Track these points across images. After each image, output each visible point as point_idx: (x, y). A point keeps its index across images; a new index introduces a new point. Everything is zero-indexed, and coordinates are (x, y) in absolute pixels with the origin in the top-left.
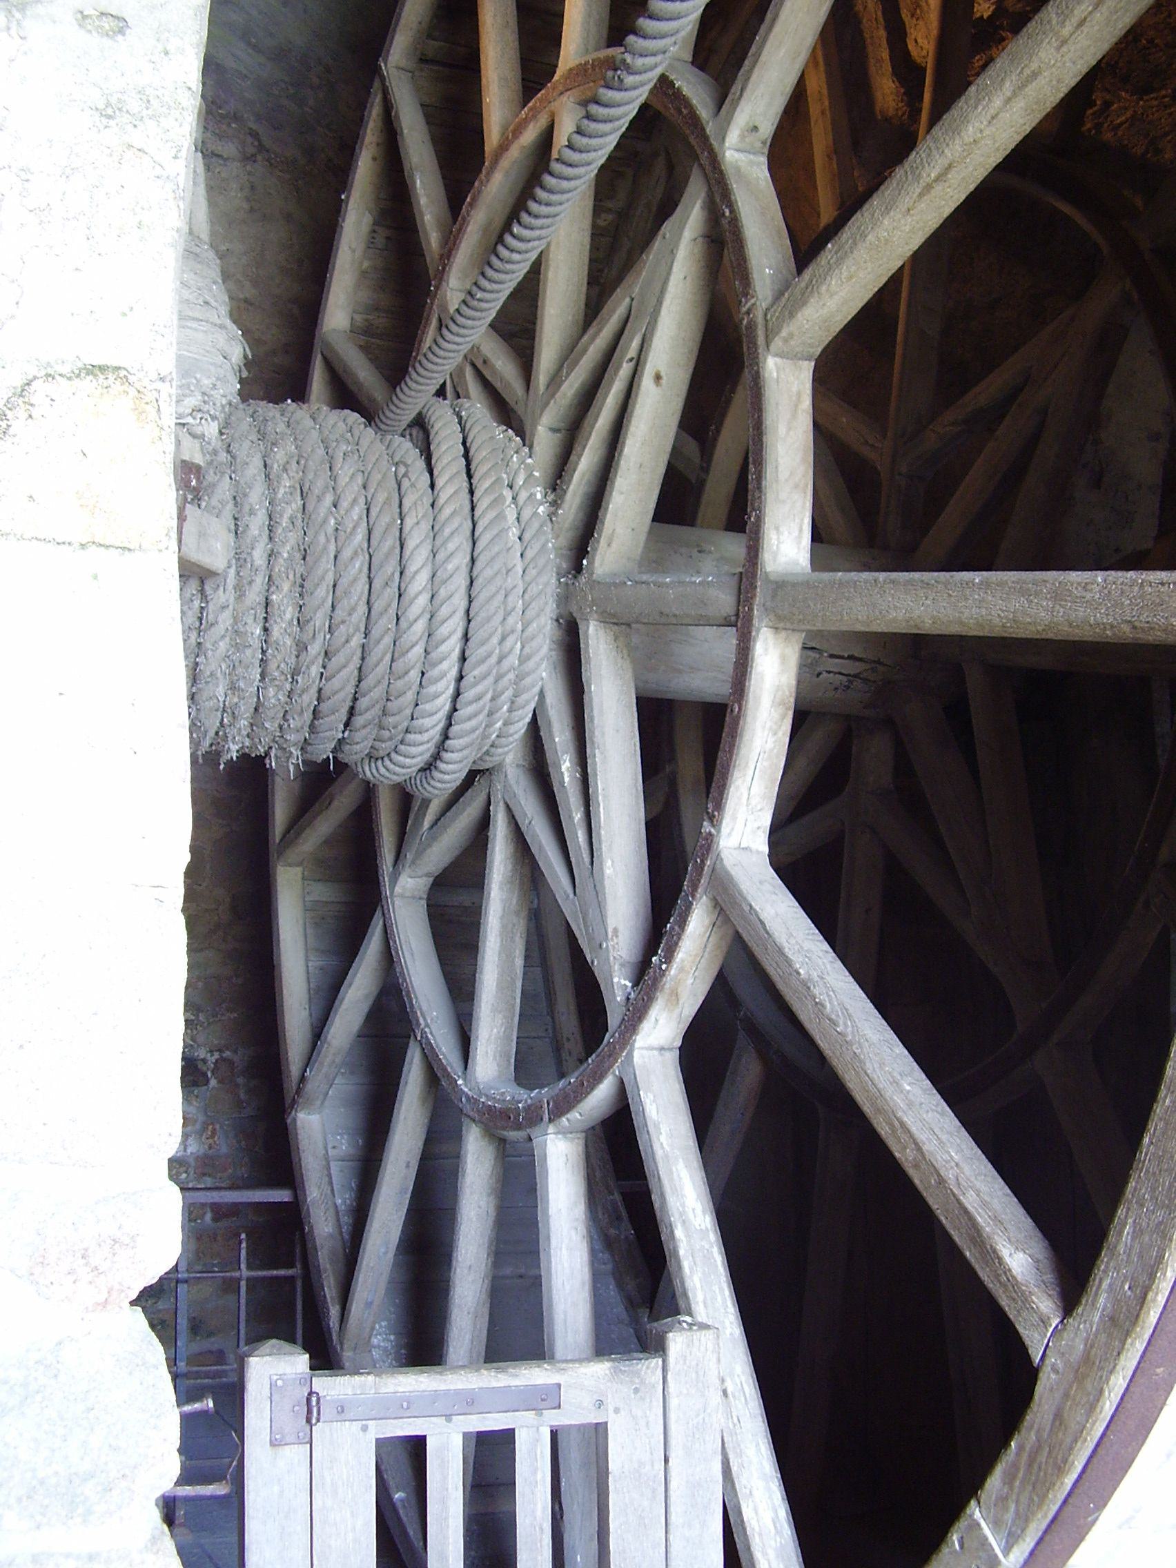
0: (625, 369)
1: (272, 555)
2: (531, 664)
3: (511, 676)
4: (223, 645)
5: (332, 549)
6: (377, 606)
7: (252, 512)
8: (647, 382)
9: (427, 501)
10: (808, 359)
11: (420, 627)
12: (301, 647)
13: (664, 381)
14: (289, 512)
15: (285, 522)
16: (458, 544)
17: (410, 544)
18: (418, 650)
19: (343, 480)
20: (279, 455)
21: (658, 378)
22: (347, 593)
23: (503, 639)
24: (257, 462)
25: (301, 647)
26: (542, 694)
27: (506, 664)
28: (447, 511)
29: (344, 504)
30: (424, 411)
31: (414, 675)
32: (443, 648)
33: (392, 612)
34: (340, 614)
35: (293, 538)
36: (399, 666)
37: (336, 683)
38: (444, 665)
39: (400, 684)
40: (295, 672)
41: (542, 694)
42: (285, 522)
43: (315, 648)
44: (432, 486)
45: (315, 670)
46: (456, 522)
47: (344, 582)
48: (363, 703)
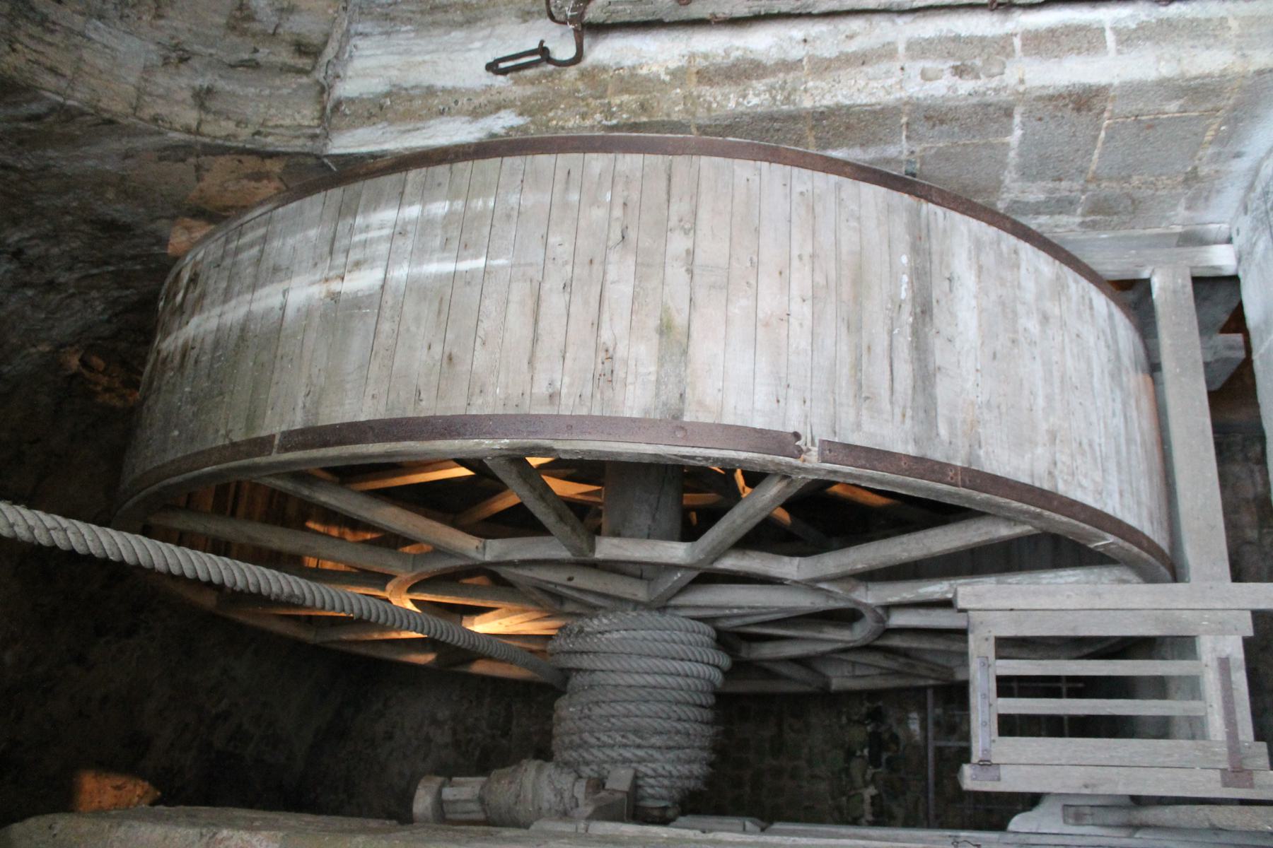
0: (559, 588)
1: (639, 747)
2: (682, 626)
3: (689, 635)
4: (679, 767)
5: (636, 719)
6: (660, 698)
7: (621, 755)
8: (571, 583)
9: (612, 675)
10: (594, 540)
11: (670, 679)
12: (678, 732)
13: (571, 575)
14: (619, 739)
15: (625, 741)
16: (636, 663)
17: (632, 682)
18: (680, 680)
19: (603, 712)
20: (593, 741)
21: (570, 579)
22: (656, 713)
23: (674, 642)
24: (595, 751)
25: (678, 732)
26: (693, 618)
27: (683, 638)
28: (618, 666)
29: (614, 712)
30: (577, 680)
31: (689, 681)
32: (679, 669)
33: (663, 692)
34: (664, 716)
35: (632, 737)
36: (685, 688)
37: (691, 715)
38: (686, 668)
39: (693, 686)
40: (688, 734)
41: (693, 618)
42: (625, 741)
43: (679, 726)
44: (602, 671)
45: (687, 726)
46: (623, 663)
47: (651, 714)
48: (698, 702)
